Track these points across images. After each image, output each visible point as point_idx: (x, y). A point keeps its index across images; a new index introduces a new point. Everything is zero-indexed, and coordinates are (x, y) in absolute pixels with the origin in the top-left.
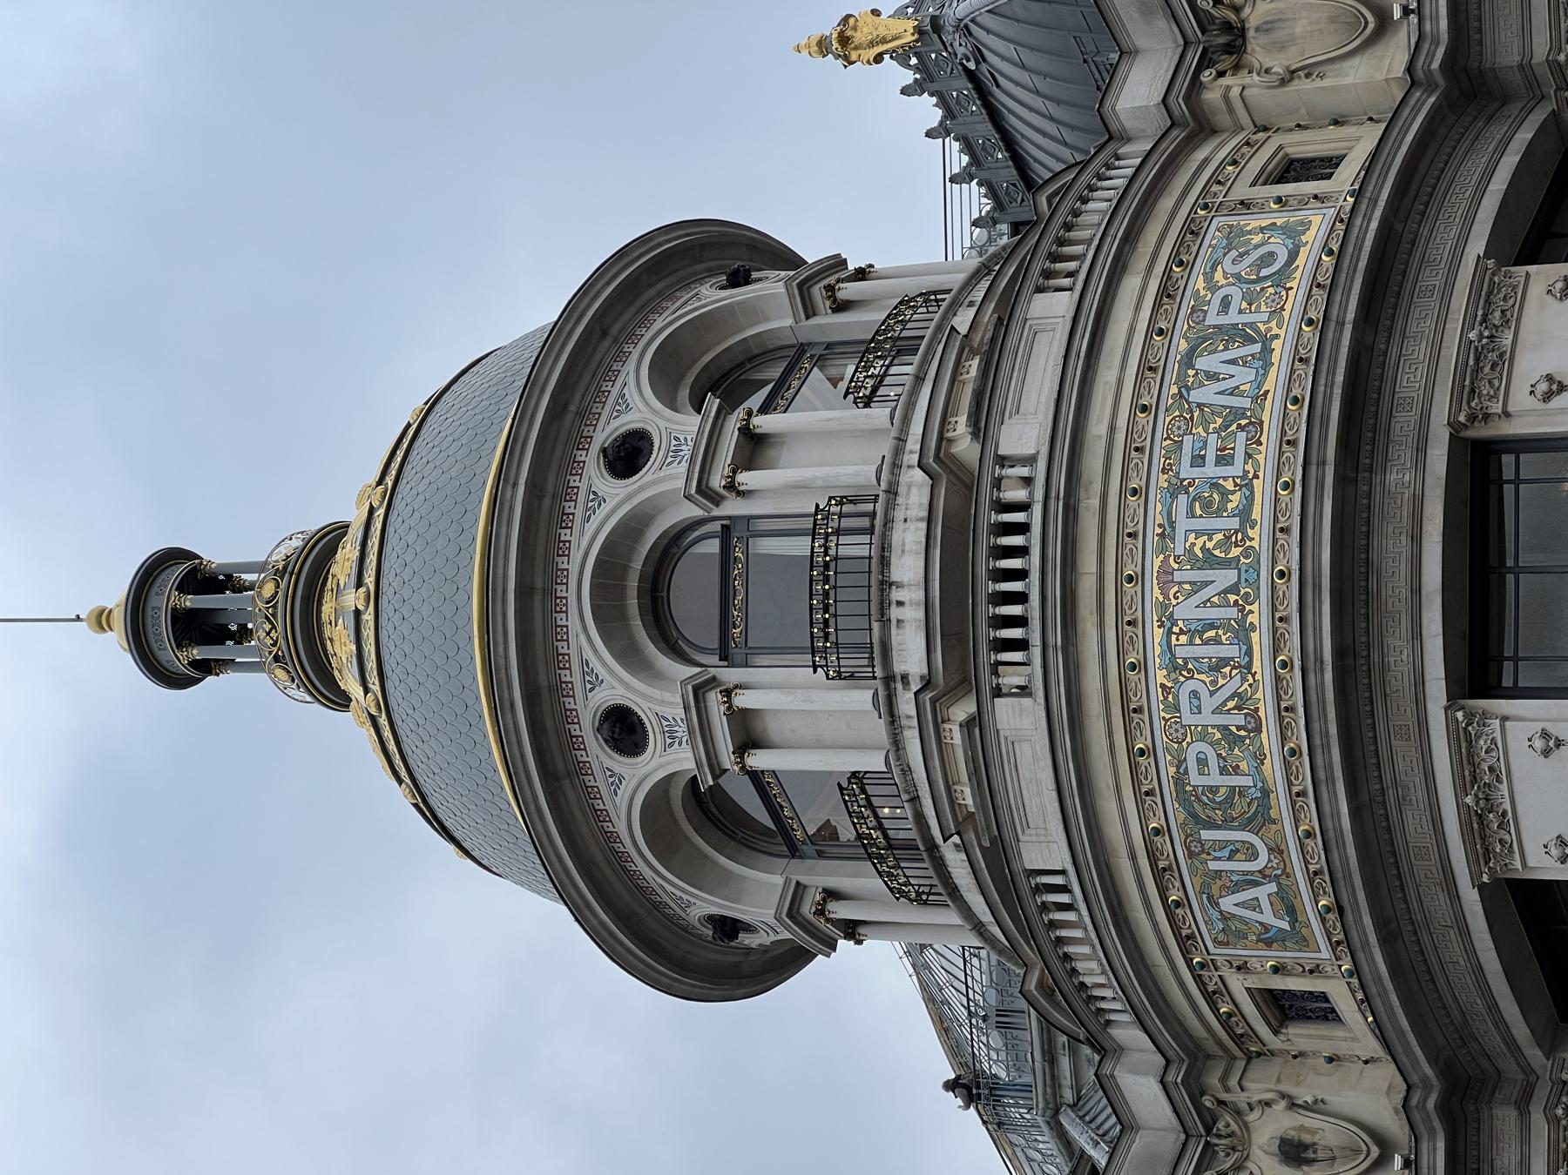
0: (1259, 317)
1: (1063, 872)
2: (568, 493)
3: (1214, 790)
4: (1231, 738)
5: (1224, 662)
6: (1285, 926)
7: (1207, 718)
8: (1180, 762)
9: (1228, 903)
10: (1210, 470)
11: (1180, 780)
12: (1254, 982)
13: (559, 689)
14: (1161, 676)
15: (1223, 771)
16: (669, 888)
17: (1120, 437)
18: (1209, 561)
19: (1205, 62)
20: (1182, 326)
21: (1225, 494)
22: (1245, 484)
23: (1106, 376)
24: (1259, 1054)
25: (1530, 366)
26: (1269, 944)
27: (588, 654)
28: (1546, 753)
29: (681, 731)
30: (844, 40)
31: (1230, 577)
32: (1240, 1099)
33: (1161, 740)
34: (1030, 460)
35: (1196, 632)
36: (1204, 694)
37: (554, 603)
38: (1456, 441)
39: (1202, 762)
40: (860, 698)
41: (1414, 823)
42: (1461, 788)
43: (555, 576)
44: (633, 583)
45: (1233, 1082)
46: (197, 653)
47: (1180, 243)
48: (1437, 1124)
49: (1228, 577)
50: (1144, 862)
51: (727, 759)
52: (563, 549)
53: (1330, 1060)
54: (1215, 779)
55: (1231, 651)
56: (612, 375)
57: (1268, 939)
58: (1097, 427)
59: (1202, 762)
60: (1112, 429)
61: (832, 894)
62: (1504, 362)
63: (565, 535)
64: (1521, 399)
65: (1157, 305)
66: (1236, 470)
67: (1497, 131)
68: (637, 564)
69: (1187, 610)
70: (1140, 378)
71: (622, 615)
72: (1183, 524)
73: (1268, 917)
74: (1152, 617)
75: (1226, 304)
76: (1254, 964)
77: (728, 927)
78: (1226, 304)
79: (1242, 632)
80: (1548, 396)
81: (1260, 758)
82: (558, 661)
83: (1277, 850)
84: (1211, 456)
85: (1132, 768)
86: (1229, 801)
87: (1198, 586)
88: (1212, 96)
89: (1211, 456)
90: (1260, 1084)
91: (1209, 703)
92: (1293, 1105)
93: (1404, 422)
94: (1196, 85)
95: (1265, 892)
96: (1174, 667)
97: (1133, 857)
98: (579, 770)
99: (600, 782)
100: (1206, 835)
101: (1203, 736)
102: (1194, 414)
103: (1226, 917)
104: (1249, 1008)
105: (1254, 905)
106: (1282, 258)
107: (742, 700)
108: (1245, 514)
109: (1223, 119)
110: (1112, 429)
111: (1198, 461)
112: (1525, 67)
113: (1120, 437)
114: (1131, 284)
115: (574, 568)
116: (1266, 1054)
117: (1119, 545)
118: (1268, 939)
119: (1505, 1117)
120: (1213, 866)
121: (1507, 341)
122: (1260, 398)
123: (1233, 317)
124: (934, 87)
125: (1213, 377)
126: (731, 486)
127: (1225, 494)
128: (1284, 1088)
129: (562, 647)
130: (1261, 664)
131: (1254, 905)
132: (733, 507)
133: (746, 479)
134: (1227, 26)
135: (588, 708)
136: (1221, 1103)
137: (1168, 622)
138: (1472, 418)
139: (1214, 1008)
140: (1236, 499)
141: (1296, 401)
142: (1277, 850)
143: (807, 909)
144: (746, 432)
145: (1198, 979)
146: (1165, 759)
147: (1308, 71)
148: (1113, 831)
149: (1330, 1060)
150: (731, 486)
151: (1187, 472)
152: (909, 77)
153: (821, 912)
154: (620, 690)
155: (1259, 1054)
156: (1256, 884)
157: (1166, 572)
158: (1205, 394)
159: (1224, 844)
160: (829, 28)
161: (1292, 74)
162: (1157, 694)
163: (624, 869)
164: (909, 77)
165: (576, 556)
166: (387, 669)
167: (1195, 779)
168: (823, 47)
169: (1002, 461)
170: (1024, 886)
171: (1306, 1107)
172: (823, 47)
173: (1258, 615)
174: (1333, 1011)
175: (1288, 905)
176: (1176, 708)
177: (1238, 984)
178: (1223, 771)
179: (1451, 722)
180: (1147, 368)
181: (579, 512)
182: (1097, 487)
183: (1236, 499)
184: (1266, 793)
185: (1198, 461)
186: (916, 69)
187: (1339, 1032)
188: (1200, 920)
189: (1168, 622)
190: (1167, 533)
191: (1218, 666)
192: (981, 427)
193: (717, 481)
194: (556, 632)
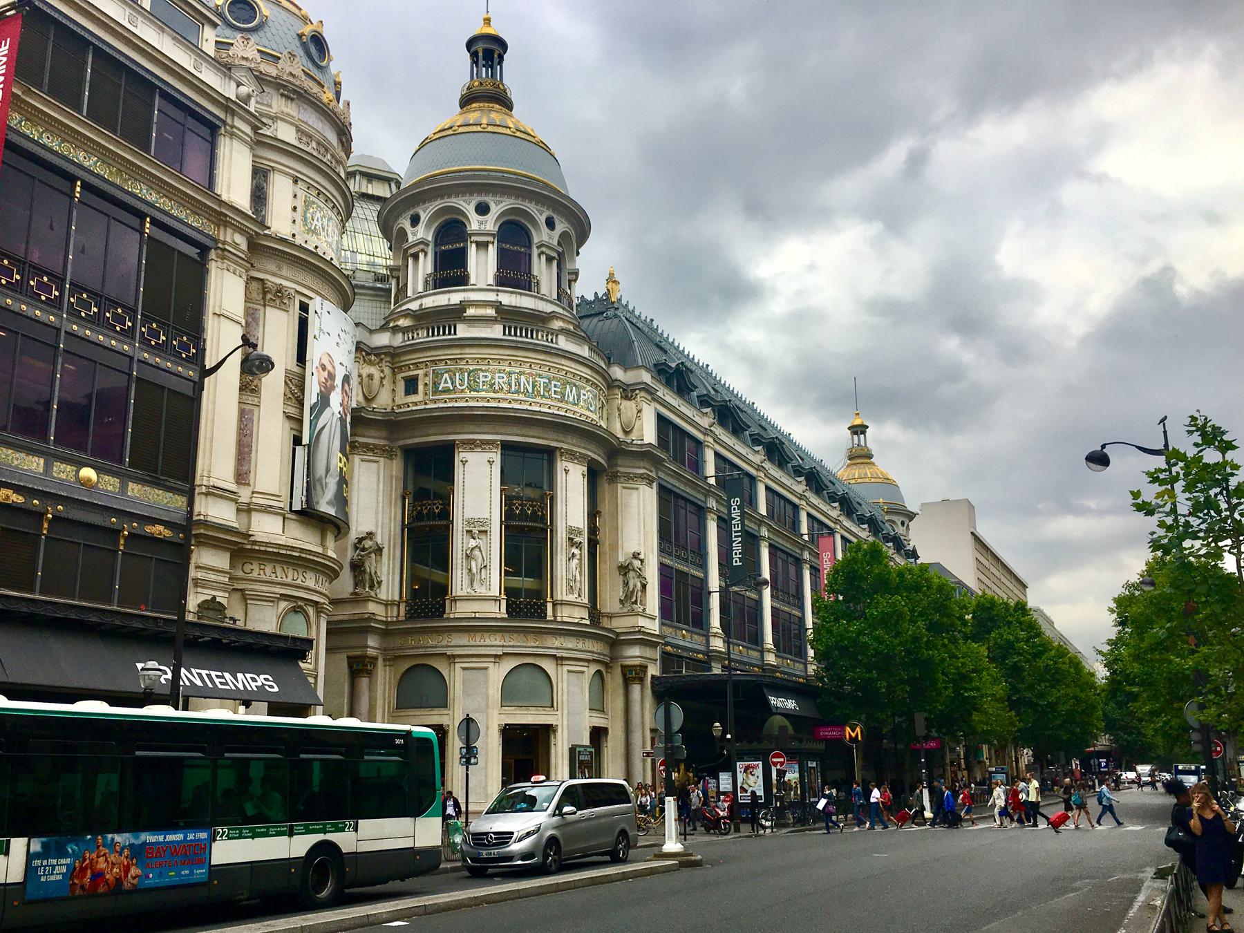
0: (582, 403)
1: (455, 334)
2: (543, 205)
3: (479, 378)
4: (492, 385)
5: (511, 387)
6: (440, 389)
7: (497, 380)
8: (485, 371)
9: (446, 375)
10: (553, 389)
11: (481, 370)
12: (421, 377)
13: (495, 194)
14: (508, 369)
15: (483, 382)
16: (431, 208)
17: (561, 367)
18: (534, 386)
19: (624, 390)
20: (581, 384)
21: (548, 392)
22: (550, 397)
23: (573, 365)
24: (394, 371)
25: (570, 466)
26: (434, 383)
27: (504, 204)
28: (489, 461)
29: (482, 227)
30: (615, 282)
31: (530, 391)
32: (384, 364)
33: (491, 367)
34: (556, 343)
35: (518, 381)
36: (504, 380)
37: (517, 197)
38: (556, 448)
39: (486, 377)
40: (491, 280)
41: (472, 428)
42: (480, 440)
43: (524, 198)
44: (518, 218)
45: (388, 364)
46: (481, 54)
47: (596, 384)
48: (387, 418)
49: (530, 391)
50: (459, 356)
51: (473, 238)
52: (530, 201)
53: (393, 390)
54: (482, 379)
55: (513, 389)
56: (569, 222)
57: (436, 384)
58: (563, 362)
59: (486, 377)
60: (563, 365)
61: (426, 254)
62: (572, 461)
63: (534, 203)
64: (565, 464)
65: (585, 378)
66: (553, 395)
67: (605, 458)
68: (523, 221)
69: (523, 379)
70: (572, 373)
71: (511, 214)
72: (542, 380)
73: (442, 385)
74: (521, 370)
75: (584, 395)
76: (427, 378)
77: (415, 221)
78: (584, 395)
79: (518, 392)
80: (565, 470)
81: (487, 391)
82: (503, 194)
83: (462, 391)
84: (556, 389)
85: (485, 359)
86: (475, 381)
87: (528, 382)
88: (618, 391)
89: (556, 389)
90: (387, 371)
91: (501, 381)
92: (382, 378)
93: (561, 437)
94: (619, 387)
95: (450, 385)
96: (510, 373)
97: (461, 354)
98: (472, 194)
99: (467, 198)
100: (466, 374)
101: (493, 378)
102: (564, 385)
103: (442, 374)
104: (411, 373)
105: (446, 382)
106: (591, 409)
107: (490, 246)
108: (544, 396)
109: (611, 392)
110: (563, 365)
111: (555, 386)
112: (617, 465)
113: (561, 367)
114: (589, 372)
115: (526, 204)
116: (394, 374)
117: (539, 364)
118: (436, 384)
119: (384, 434)
120: (457, 374)
121: (576, 461)
122: (567, 402)
123: (582, 396)
124: (596, 301)
125: (571, 392)
126: (543, 253)
127: (548, 392)
128: (387, 377)
129: (506, 196)
130: (509, 396)
131: (446, 382)
132: (535, 252)
133: (543, 258)
134: (632, 396)
135: (490, 200)
136: (382, 359)
137: (521, 373)
138: (562, 453)
139: (412, 364)
140: (547, 394)
141: (566, 411)
142: (462, 391)
143: (422, 246)
144: (554, 258)
145: (422, 362)
146: (487, 367)
147: (619, 414)
148: (467, 350)
149: (393, 390)
150: (543, 253)
151: (553, 383)
152: (600, 295)
153: (422, 250)
154: (495, 211)
155: (394, 371)
156: (452, 384)
157: (532, 375)
158: (568, 389)
159: (464, 378)
160: (617, 278)
161: (619, 409)
162: (503, 368)
163: (438, 197)
164: (600, 295)
165: (529, 205)
166: (496, 135)
167: (481, 374)
168: (612, 275)
169: (557, 336)
170: (452, 323)
171: (381, 382)
172: (612, 275)
173: (521, 397)
174: (410, 394)
175: (446, 391)
176: (500, 372)
177: (420, 372)
178: (483, 382)
179: (497, 441)
180: (574, 374)
181: (538, 208)
182: (551, 360)
183: (547, 394)
184: (478, 392)
185: (555, 386)
186: (602, 297)
187: (403, 394)
188: (441, 366)
189: (521, 373)
190: (540, 376)
191: (510, 385)
192: (563, 331)
193: (544, 249)
194: (510, 196)
